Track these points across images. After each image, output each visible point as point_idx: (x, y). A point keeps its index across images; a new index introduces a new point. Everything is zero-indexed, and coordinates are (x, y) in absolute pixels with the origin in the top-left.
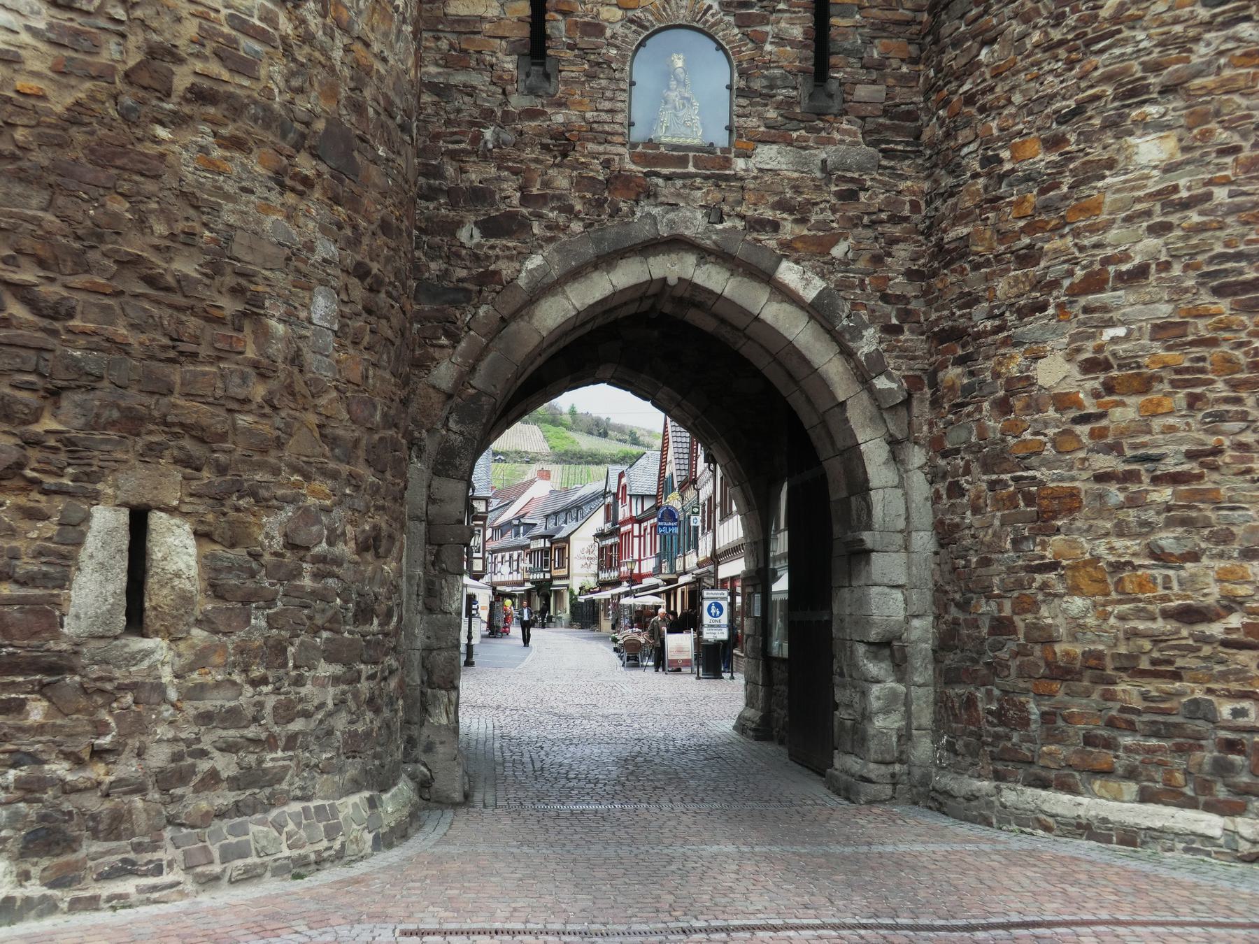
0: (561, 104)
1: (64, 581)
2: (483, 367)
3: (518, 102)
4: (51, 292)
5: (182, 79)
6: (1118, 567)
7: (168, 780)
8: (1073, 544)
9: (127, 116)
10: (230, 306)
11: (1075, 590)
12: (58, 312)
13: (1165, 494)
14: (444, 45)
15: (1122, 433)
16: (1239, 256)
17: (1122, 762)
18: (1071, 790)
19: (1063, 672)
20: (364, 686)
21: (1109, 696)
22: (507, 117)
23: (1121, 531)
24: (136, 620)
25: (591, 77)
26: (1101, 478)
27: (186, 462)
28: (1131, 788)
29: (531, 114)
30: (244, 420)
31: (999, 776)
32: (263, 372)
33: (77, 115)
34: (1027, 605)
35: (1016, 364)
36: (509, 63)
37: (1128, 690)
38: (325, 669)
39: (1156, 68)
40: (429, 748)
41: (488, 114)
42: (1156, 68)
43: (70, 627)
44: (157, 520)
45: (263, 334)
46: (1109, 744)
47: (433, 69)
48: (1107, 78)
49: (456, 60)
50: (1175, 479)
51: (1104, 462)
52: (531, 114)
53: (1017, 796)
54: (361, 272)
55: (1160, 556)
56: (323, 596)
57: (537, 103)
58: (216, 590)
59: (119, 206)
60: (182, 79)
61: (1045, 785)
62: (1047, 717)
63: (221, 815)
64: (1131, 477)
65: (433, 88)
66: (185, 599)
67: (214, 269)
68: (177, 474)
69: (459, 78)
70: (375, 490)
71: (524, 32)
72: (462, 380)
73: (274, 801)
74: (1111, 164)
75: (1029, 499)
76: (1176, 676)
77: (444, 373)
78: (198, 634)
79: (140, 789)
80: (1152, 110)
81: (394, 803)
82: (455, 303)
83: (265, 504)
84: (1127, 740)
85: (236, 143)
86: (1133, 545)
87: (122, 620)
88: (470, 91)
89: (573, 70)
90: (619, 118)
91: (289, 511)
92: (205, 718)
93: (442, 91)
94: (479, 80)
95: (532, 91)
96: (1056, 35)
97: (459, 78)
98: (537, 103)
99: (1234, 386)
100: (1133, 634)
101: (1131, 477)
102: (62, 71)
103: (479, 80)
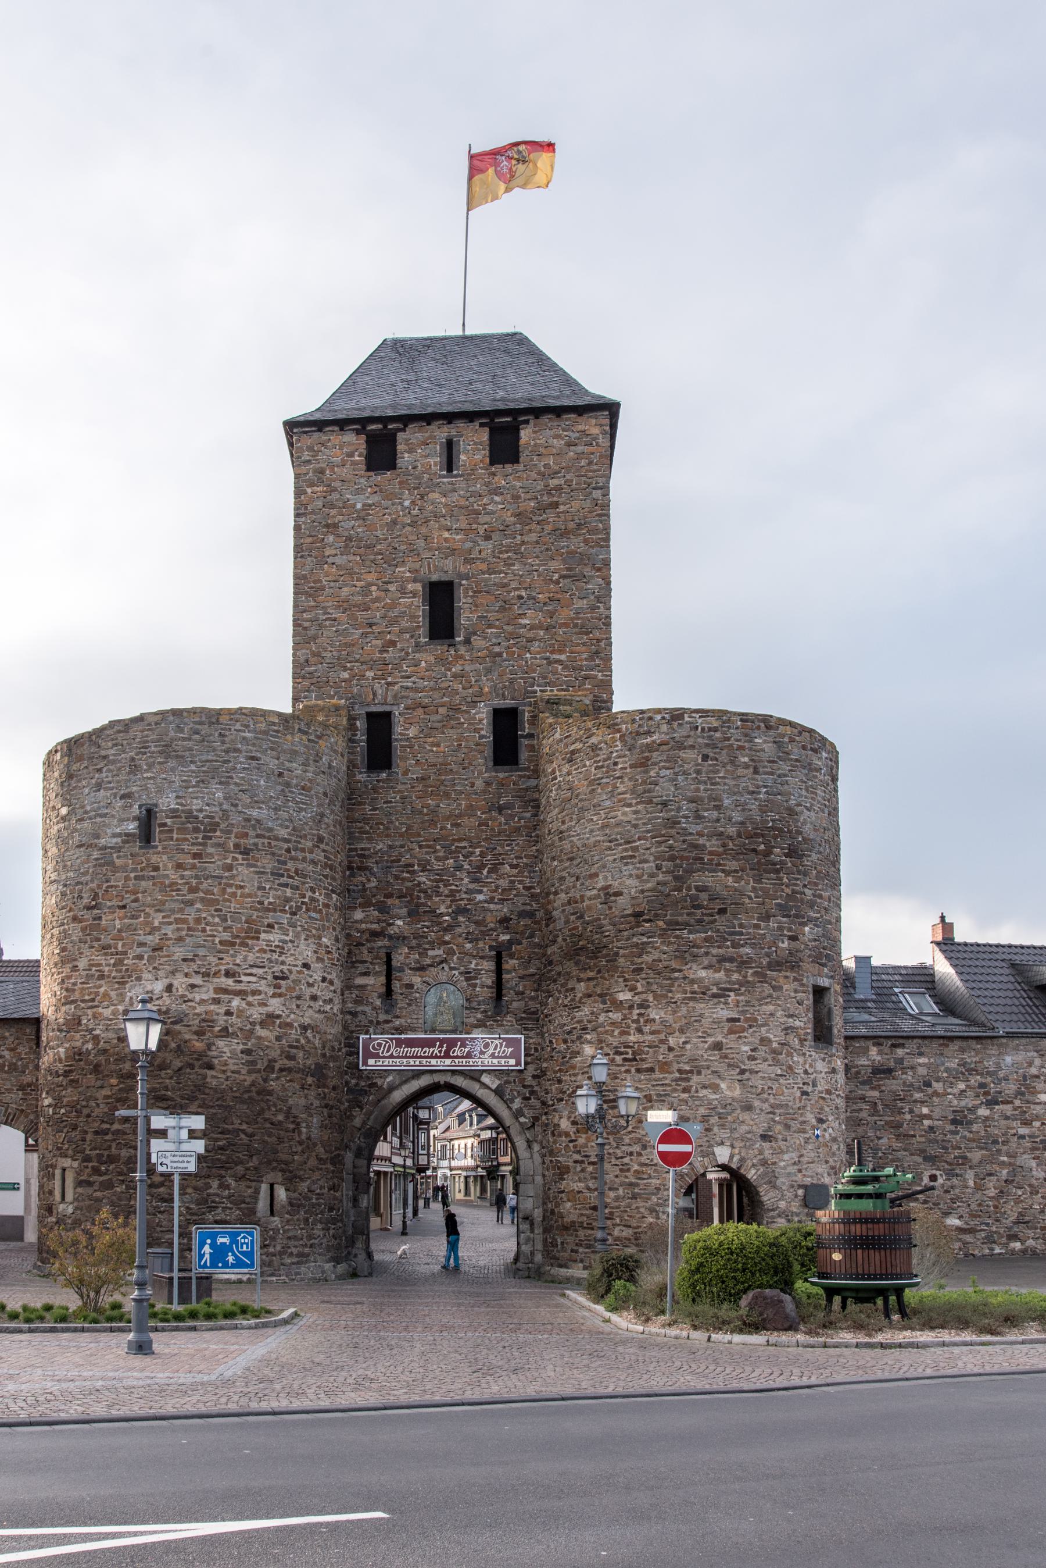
0: (397, 1017)
1: (256, 1203)
2: (372, 1117)
3: (382, 1017)
4: (250, 1130)
5: (277, 1066)
6: (579, 1192)
7: (281, 1254)
8: (568, 1184)
9: (265, 1080)
10: (292, 1126)
11: (569, 1200)
12: (252, 1135)
13: (590, 1169)
14: (354, 996)
15: (581, 1147)
16: (609, 1091)
17: (581, 1256)
18: (567, 1268)
19: (566, 1228)
20: (332, 1232)
21: (577, 1236)
22: (378, 1023)
23: (580, 1180)
24: (272, 1214)
25: (409, 1005)
26: (576, 1162)
27: (282, 1170)
28: (581, 1265)
29: (387, 1022)
30: (296, 1158)
31: (552, 1265)
32: (300, 1143)
33: (253, 1084)
34: (557, 1205)
35: (556, 1121)
36: (378, 1002)
37: (581, 1233)
38: (319, 1226)
39: (589, 1022)
40: (356, 1256)
41: (371, 1022)
42: (589, 1022)
43: (259, 1215)
44: (276, 1186)
45: (300, 1133)
46: (577, 1252)
47: (350, 1005)
48: (578, 1022)
49: (358, 1002)
50: (593, 1163)
51: (577, 1157)
52: (387, 1022)
53: (556, 1271)
54: (326, 1106)
55: (589, 1189)
56: (319, 1205)
57: (389, 1017)
58: (291, 1204)
59: (263, 1105)
60: (277, 1066)
61: (561, 1266)
62: (562, 1243)
63: (293, 1263)
64: (582, 1162)
65: (350, 1013)
66: (284, 1207)
67: (287, 1117)
68: (280, 1174)
69: (360, 1009)
70: (333, 1172)
71: (383, 990)
72: (364, 1123)
73: (306, 1262)
74: (578, 1053)
75: (559, 1168)
76: (592, 1229)
77: (357, 1122)
78: (287, 1216)
79: (275, 1255)
80: (588, 1037)
81: (341, 1268)
82: (361, 1095)
83: (302, 1180)
84: (581, 1250)
85: (290, 1081)
86: (582, 1185)
87: (269, 1213)
88: (364, 1013)
89: (402, 1004)
90: (421, 1021)
91: (309, 1182)
92: (289, 1238)
93: (354, 1014)
94: (368, 1009)
95: (387, 1012)
96: (566, 1002)
97: (360, 1009)
98: (389, 1017)
99: (608, 1134)
100: (582, 1215)
101: (582, 1162)
102: (249, 1072)
103: (368, 1009)
